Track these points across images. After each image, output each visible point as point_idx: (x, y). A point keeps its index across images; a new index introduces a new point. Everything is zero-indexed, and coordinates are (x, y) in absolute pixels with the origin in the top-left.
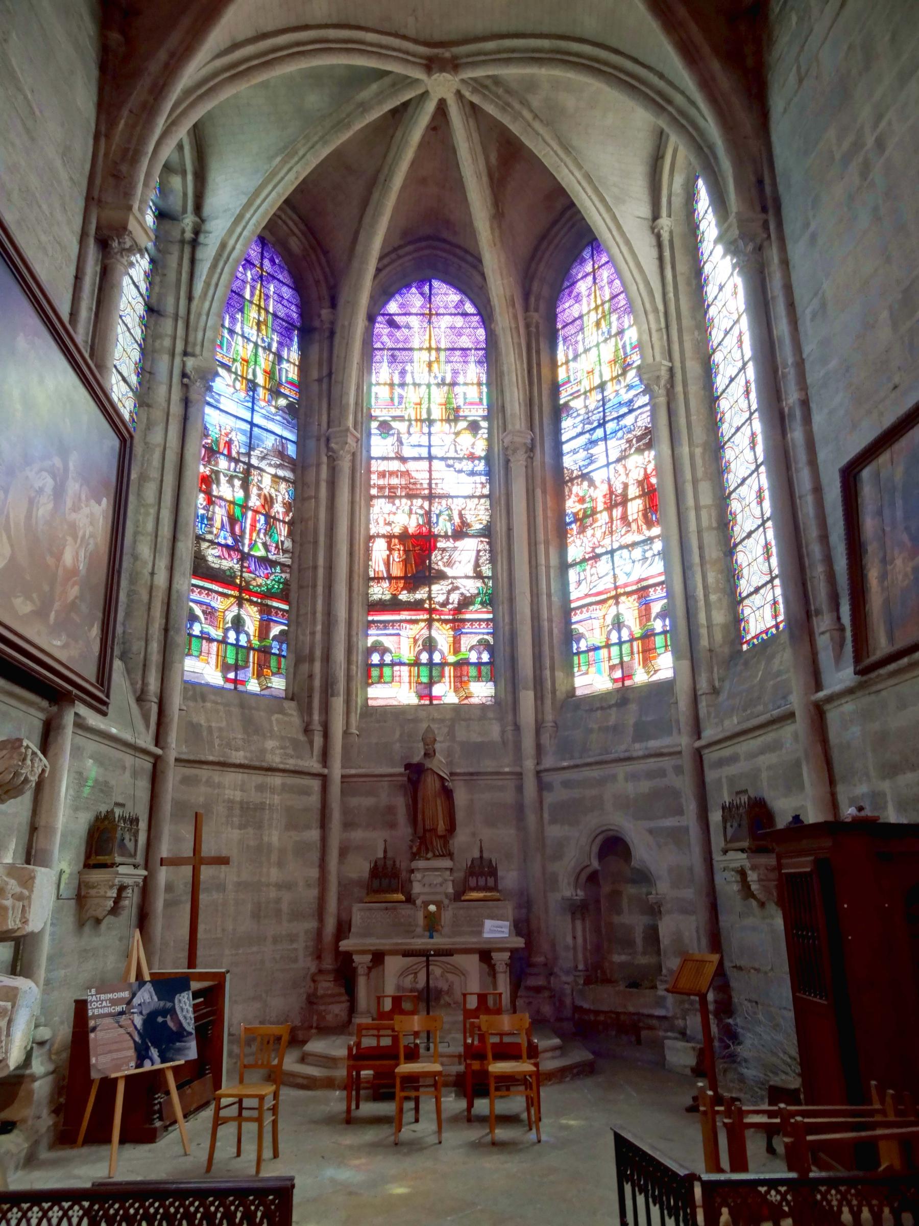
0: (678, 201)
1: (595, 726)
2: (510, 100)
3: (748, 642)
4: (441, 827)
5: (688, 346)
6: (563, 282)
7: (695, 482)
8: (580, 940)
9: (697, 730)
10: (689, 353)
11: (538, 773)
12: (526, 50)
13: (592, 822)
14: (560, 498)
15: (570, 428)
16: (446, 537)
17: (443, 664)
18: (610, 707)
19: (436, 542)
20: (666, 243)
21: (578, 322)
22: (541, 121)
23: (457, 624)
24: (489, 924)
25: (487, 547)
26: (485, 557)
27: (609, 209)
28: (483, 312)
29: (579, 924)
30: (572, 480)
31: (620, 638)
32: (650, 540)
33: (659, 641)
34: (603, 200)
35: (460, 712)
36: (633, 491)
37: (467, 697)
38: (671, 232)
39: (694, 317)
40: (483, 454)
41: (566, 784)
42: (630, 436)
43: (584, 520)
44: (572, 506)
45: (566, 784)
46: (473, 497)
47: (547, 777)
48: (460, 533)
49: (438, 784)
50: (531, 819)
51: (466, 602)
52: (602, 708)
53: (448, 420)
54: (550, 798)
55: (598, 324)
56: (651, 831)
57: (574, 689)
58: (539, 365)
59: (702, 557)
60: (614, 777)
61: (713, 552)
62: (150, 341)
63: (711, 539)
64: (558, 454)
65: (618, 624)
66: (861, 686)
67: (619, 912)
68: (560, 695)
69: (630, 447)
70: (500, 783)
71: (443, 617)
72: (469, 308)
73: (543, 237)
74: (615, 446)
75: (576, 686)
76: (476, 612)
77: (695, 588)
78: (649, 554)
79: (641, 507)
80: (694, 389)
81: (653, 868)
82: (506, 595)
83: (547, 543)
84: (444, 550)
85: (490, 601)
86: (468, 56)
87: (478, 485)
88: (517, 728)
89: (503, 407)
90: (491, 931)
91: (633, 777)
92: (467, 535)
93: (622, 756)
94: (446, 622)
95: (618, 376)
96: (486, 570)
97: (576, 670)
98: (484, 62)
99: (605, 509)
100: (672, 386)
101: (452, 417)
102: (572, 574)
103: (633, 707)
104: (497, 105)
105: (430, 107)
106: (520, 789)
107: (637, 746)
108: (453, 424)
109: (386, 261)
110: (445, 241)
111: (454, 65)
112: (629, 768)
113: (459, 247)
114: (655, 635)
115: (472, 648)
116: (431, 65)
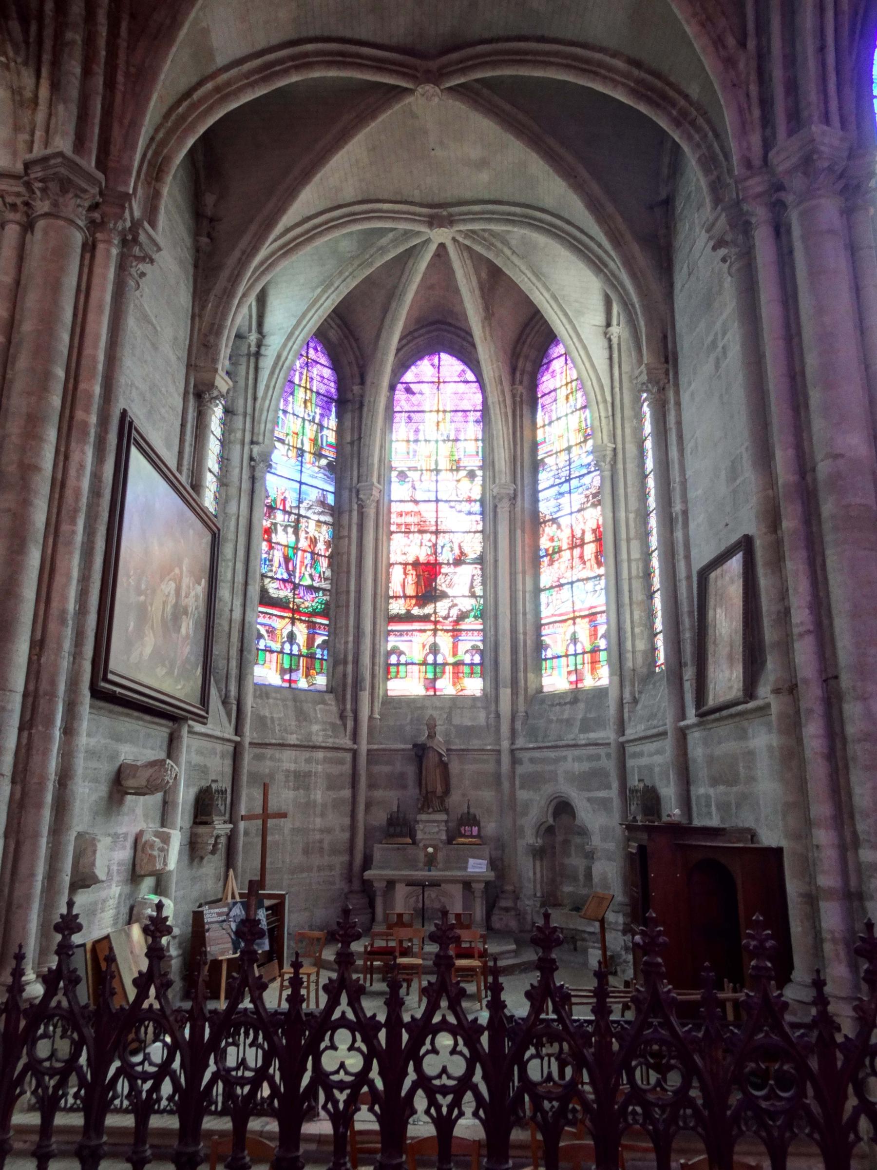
1: (555, 718)
2: (494, 240)
3: (659, 666)
4: (439, 790)
5: (628, 431)
6: (542, 360)
7: (628, 541)
8: (538, 875)
9: (621, 729)
10: (628, 438)
11: (512, 751)
12: (503, 213)
13: (548, 789)
14: (536, 536)
15: (544, 478)
16: (448, 564)
17: (445, 664)
18: (566, 704)
19: (440, 568)
20: (615, 346)
21: (553, 394)
22: (518, 256)
23: (456, 633)
24: (471, 861)
25: (480, 572)
26: (478, 580)
27: (570, 321)
29: (538, 863)
30: (545, 522)
31: (575, 650)
32: (600, 576)
34: (566, 315)
35: (455, 701)
36: (589, 537)
37: (462, 690)
38: (619, 337)
39: (633, 409)
40: (478, 497)
41: (532, 760)
42: (588, 492)
43: (554, 554)
44: (544, 543)
46: (470, 532)
47: (519, 755)
48: (459, 562)
49: (437, 759)
50: (506, 784)
51: (463, 616)
52: (559, 704)
53: (451, 470)
54: (520, 770)
55: (567, 398)
57: (542, 687)
58: (522, 427)
59: (630, 598)
60: (565, 758)
61: (639, 596)
62: (227, 434)
63: (637, 585)
64: (535, 501)
65: (574, 640)
67: (569, 855)
68: (531, 690)
69: (588, 501)
70: (485, 757)
71: (445, 628)
72: (470, 376)
73: (526, 325)
74: (578, 499)
75: (543, 684)
76: (470, 624)
78: (598, 588)
79: (594, 550)
80: (631, 466)
81: (589, 827)
82: (492, 613)
83: (524, 573)
84: (446, 574)
85: (482, 615)
86: (460, 215)
87: (475, 523)
88: (498, 716)
89: (493, 462)
90: (473, 867)
91: (579, 759)
92: (465, 563)
93: (571, 743)
94: (447, 631)
95: (581, 443)
96: (479, 591)
97: (543, 672)
98: (473, 220)
99: (569, 549)
100: (615, 462)
101: (454, 467)
102: (543, 596)
103: (582, 705)
104: (483, 246)
105: (433, 247)
106: (498, 762)
107: (582, 736)
108: (455, 473)
109: (404, 342)
110: (450, 325)
111: (450, 221)
112: (577, 752)
113: (461, 329)
114: (600, 650)
115: (467, 652)
116: (433, 221)
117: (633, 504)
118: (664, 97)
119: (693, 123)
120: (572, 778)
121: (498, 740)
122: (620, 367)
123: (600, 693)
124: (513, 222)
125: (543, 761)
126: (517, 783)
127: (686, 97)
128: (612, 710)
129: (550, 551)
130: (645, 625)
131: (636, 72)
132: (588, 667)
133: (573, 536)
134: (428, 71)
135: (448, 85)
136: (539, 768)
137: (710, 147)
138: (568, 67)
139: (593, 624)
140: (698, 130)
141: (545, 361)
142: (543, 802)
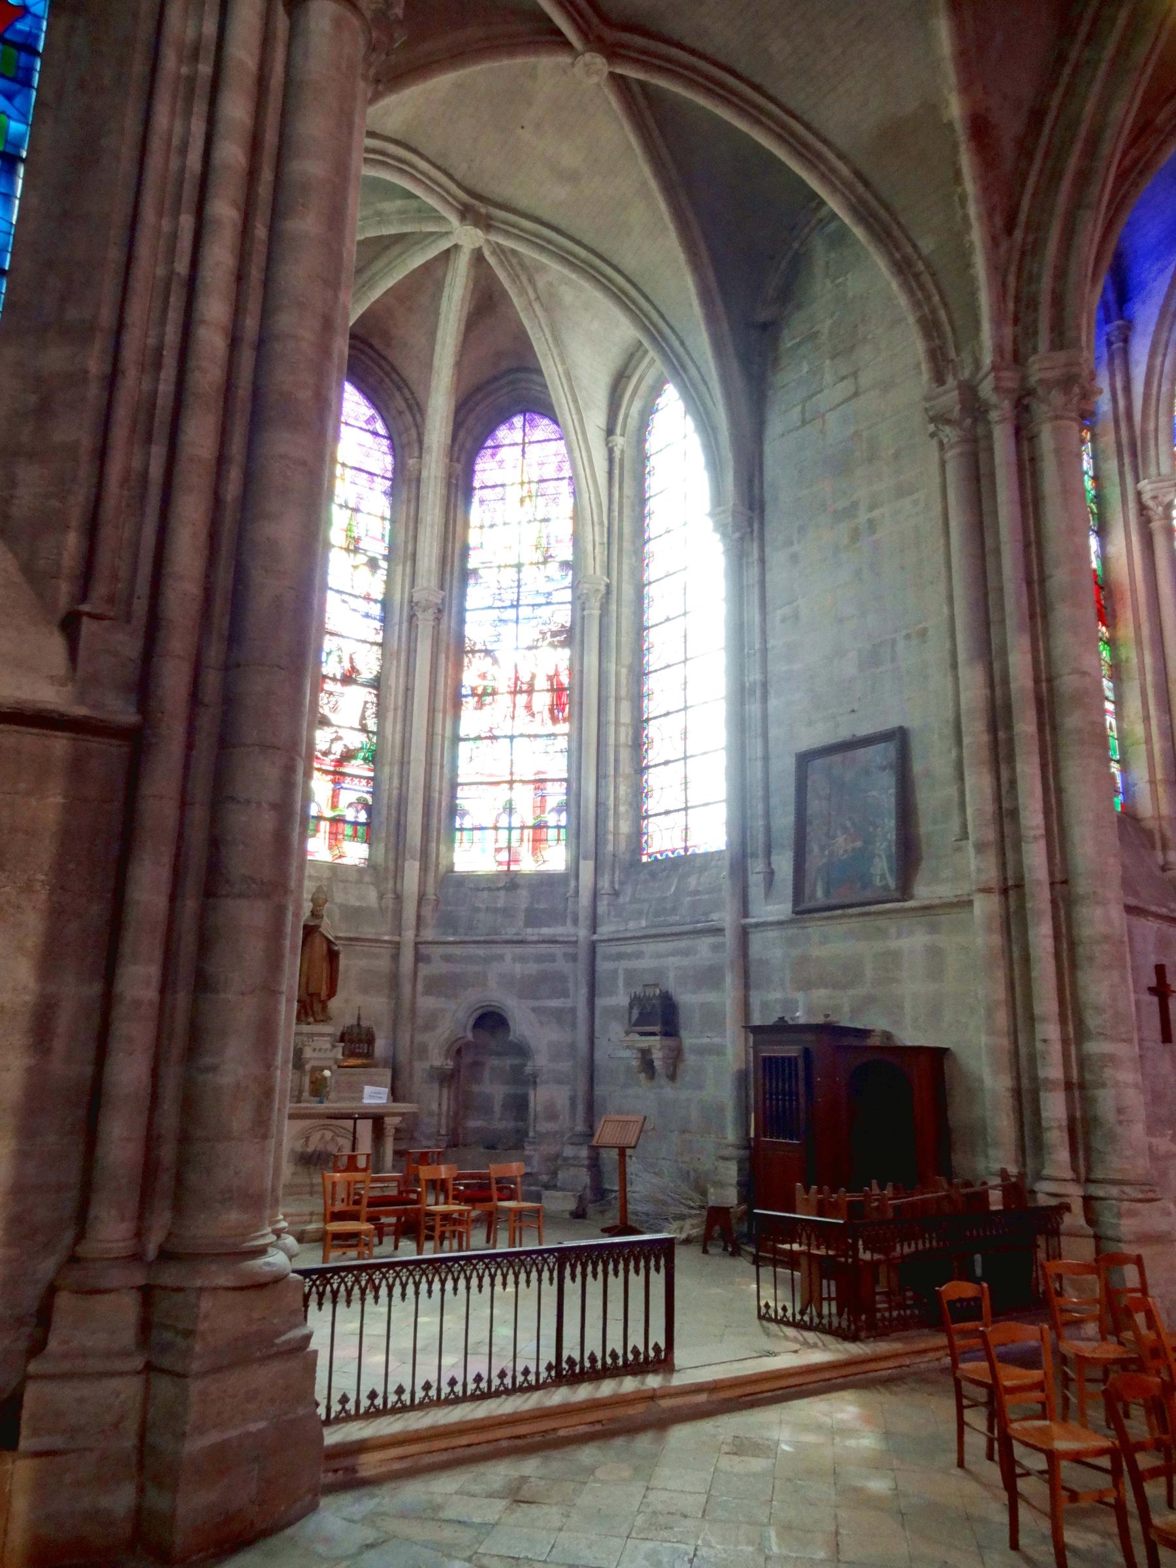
0: (633, 423)
2: (520, 272)
3: (650, 855)
4: (324, 993)
6: (485, 441)
8: (445, 1107)
11: (417, 944)
12: (561, 248)
14: (459, 667)
15: (476, 595)
16: (334, 679)
17: (319, 818)
18: (498, 889)
19: (324, 682)
20: (617, 460)
21: (499, 489)
22: (542, 305)
23: (338, 776)
24: (368, 1089)
25: (375, 700)
26: (371, 710)
28: (395, 437)
29: (445, 1092)
30: (473, 652)
31: (510, 823)
32: (554, 735)
33: (552, 834)
34: (575, 401)
35: (335, 870)
36: (542, 683)
37: (340, 857)
38: (622, 451)
39: (633, 543)
40: (380, 597)
41: (447, 958)
42: (545, 628)
43: (483, 696)
44: (470, 678)
45: (447, 958)
46: (365, 642)
48: (348, 679)
49: (325, 946)
50: (406, 989)
51: (348, 756)
52: (489, 889)
53: (347, 550)
54: (424, 970)
55: (522, 501)
56: (534, 1010)
57: (453, 864)
58: (455, 521)
59: (616, 769)
60: (502, 957)
61: (626, 768)
63: (625, 754)
64: (462, 622)
65: (509, 809)
66: (791, 921)
67: (478, 1081)
68: (442, 869)
69: (544, 639)
70: (377, 950)
71: (324, 767)
72: (380, 427)
73: (478, 389)
74: (529, 633)
75: (455, 861)
76: (356, 767)
77: (608, 798)
78: (551, 749)
79: (548, 702)
80: (627, 612)
81: (533, 1044)
84: (331, 694)
85: (374, 758)
86: (504, 222)
87: (371, 630)
88: (398, 898)
89: (414, 554)
90: (371, 1097)
91: (522, 959)
92: (355, 682)
93: (515, 938)
94: (326, 772)
95: (538, 563)
96: (372, 725)
97: (457, 845)
98: (519, 238)
99: (511, 693)
101: (352, 547)
102: (463, 747)
103: (524, 893)
104: (509, 275)
105: (445, 245)
106: (396, 958)
107: (529, 930)
108: (352, 555)
110: (371, 346)
111: (485, 224)
112: (518, 950)
113: (384, 358)
114: (548, 827)
115: (350, 805)
116: (466, 213)
117: (626, 658)
118: (889, 234)
119: (917, 276)
120: (508, 982)
121: (398, 928)
122: (621, 488)
123: (545, 883)
125: (470, 959)
126: (420, 987)
127: (914, 246)
128: (585, 899)
129: (479, 691)
130: (631, 804)
131: (860, 188)
132: (527, 846)
133: (517, 679)
134: (600, 39)
135: (619, 71)
136: (457, 968)
137: (933, 311)
138: (780, 137)
139: (540, 793)
140: (922, 287)
141: (489, 443)
142: (460, 1014)
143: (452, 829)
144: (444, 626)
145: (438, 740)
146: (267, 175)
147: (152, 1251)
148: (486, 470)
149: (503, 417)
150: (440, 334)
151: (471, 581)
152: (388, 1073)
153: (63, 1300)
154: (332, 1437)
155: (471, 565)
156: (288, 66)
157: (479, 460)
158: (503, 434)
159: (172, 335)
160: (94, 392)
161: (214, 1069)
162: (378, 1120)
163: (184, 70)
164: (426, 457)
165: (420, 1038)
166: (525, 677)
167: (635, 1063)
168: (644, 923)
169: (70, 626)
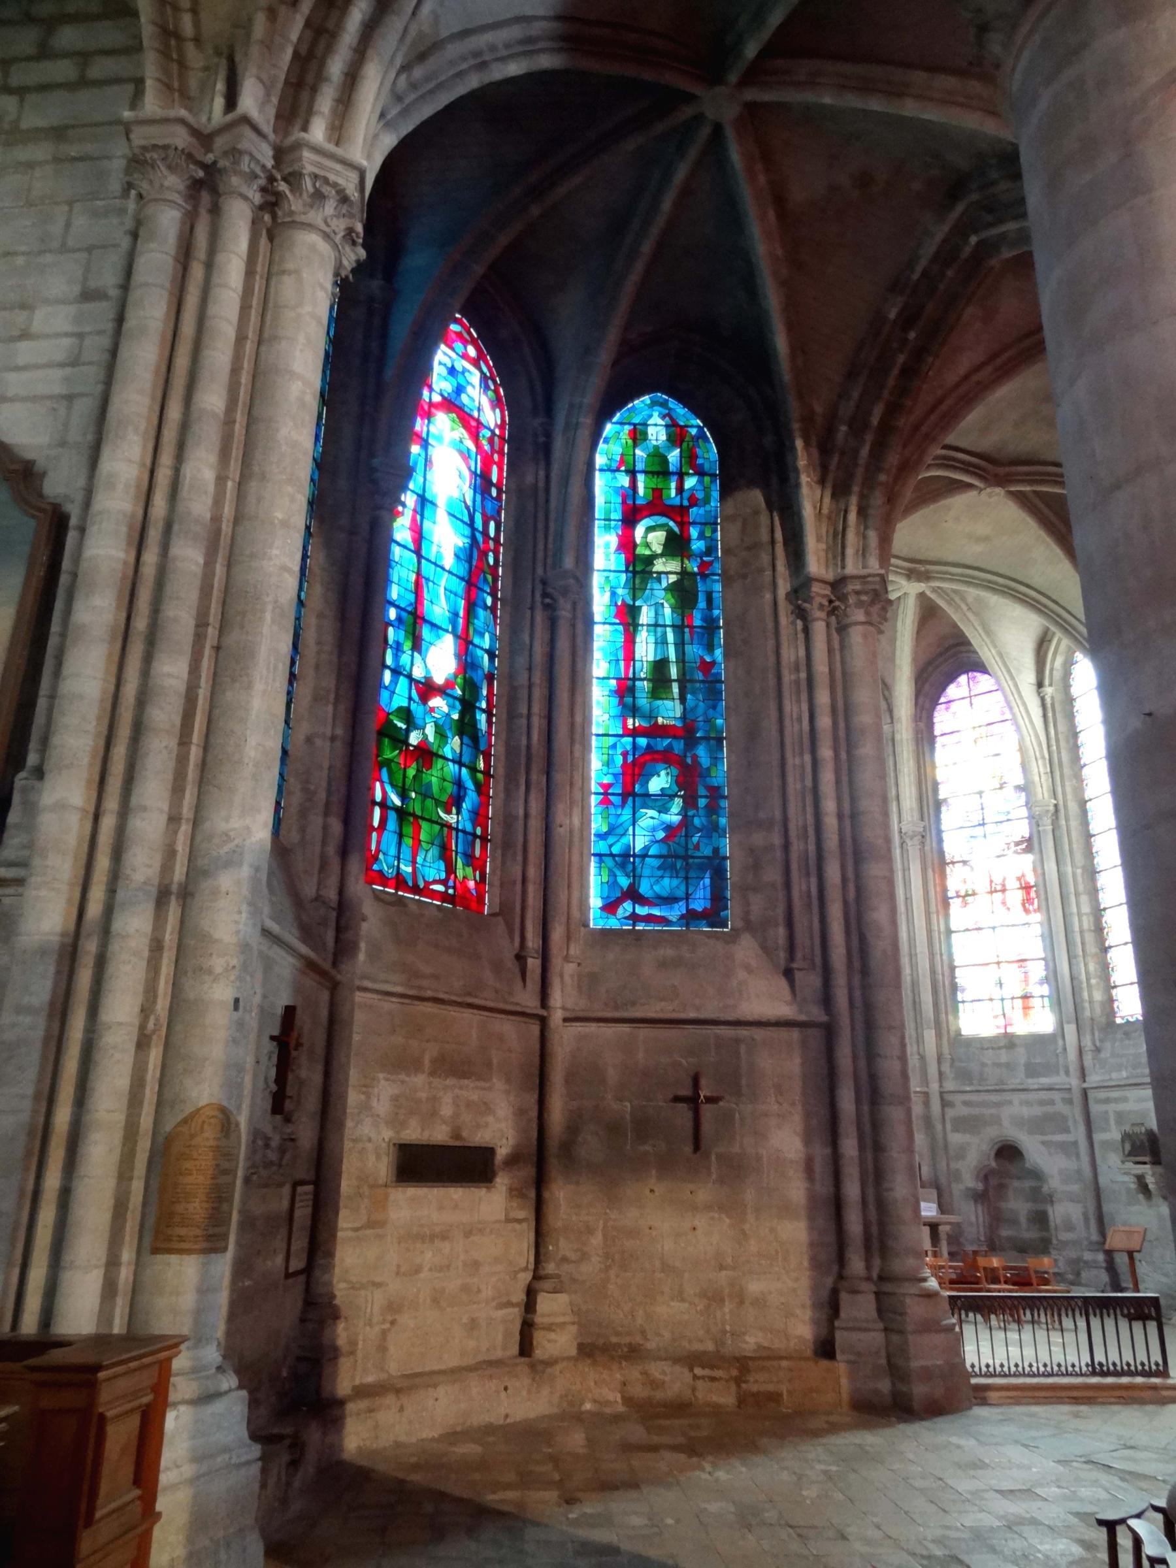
0: (1058, 675)
1: (989, 1062)
3: (1122, 1018)
5: (1068, 789)
6: (939, 698)
7: (1077, 895)
8: (981, 1219)
9: (1083, 1076)
10: (1069, 797)
11: (941, 1093)
14: (943, 876)
15: (949, 819)
18: (999, 1048)
20: (1049, 705)
27: (1012, 678)
30: (953, 863)
33: (1035, 1002)
34: (1009, 671)
36: (1012, 884)
38: (1052, 698)
41: (966, 1103)
42: (1009, 840)
54: (950, 1113)
56: (1043, 1143)
60: (1010, 1102)
61: (1092, 949)
63: (1090, 938)
64: (940, 841)
68: (952, 1034)
77: (1080, 974)
80: (1074, 824)
83: (937, 912)
86: (937, 572)
91: (1028, 1103)
100: (1057, 818)
104: (946, 601)
107: (1030, 1081)
111: (925, 577)
112: (1023, 1096)
117: (1079, 859)
120: (1020, 1122)
122: (1055, 726)
123: (1037, 1041)
124: (969, 583)
126: (948, 1126)
128: (1072, 1055)
129: (962, 893)
130: (1100, 977)
132: (1019, 1011)
133: (991, 882)
134: (996, 475)
135: (1012, 489)
136: (976, 1111)
139: (1023, 970)
141: (942, 700)
142: (984, 1147)
143: (955, 1003)
144: (927, 848)
145: (936, 935)
146: (842, 725)
147: (875, 1275)
148: (942, 719)
149: (951, 678)
150: (898, 643)
151: (944, 809)
152: (934, 1193)
153: (844, 1296)
154: (973, 1381)
155: (941, 797)
156: (843, 662)
157: (936, 714)
158: (952, 691)
159: (810, 819)
160: (779, 854)
161: (891, 1189)
162: (934, 1227)
163: (793, 677)
164: (897, 726)
165: (953, 1165)
166: (998, 880)
167: (1133, 1186)
168: (1124, 1074)
169: (788, 974)
